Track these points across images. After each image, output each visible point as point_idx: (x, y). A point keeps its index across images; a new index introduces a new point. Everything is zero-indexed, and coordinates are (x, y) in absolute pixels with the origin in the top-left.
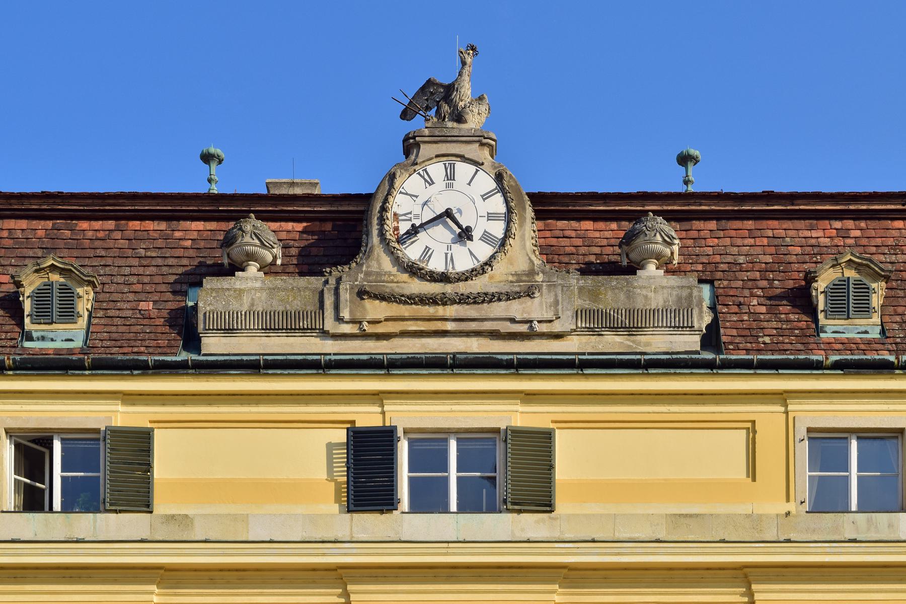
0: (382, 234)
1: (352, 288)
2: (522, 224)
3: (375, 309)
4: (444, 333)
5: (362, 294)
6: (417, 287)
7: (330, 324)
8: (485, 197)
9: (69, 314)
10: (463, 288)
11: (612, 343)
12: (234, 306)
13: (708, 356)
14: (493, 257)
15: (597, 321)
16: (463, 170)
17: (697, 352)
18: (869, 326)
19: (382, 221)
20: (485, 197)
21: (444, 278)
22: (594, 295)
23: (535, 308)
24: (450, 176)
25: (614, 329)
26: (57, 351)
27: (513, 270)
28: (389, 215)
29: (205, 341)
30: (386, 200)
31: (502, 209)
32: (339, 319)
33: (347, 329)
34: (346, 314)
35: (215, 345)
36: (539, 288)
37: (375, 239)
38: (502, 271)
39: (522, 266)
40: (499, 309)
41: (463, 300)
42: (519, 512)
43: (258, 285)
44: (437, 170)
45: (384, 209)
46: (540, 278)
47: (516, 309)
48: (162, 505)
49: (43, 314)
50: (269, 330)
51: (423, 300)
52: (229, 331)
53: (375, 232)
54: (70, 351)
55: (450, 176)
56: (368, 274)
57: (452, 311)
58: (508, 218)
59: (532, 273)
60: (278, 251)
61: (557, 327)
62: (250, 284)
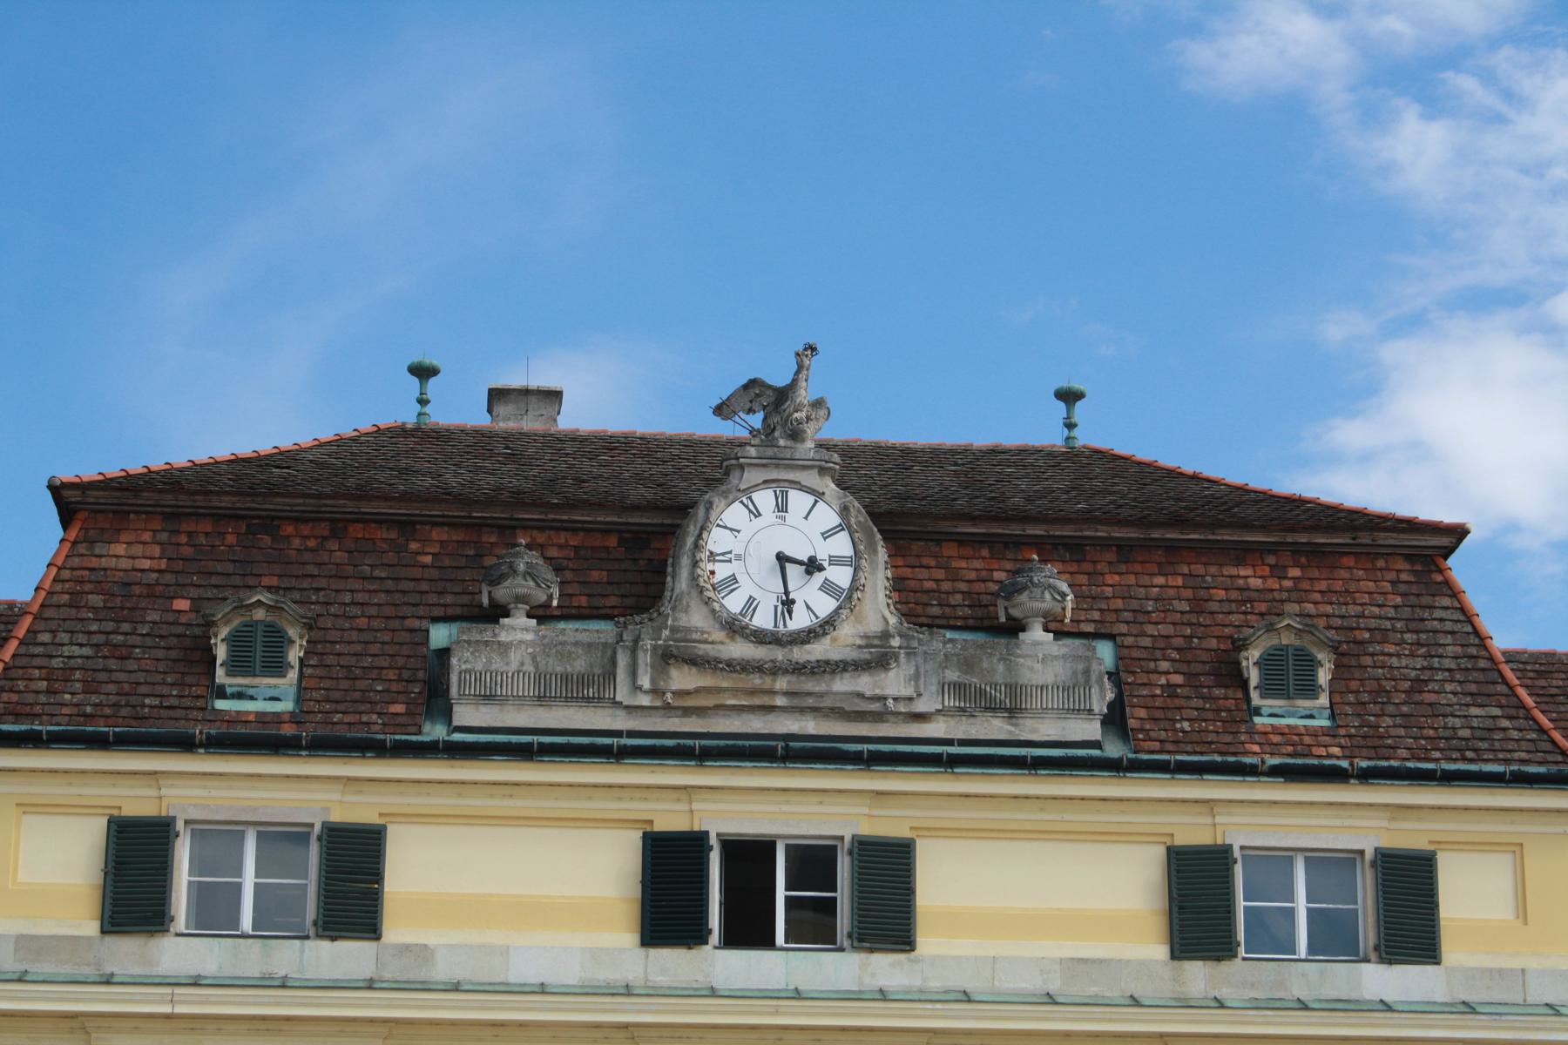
0: (694, 578)
1: (655, 648)
2: (874, 571)
3: (682, 679)
4: (772, 709)
5: (667, 658)
6: (740, 650)
7: (622, 694)
8: (826, 535)
9: (276, 666)
10: (801, 654)
11: (995, 727)
12: (498, 664)
13: (1114, 750)
14: (837, 612)
15: (973, 699)
16: (794, 495)
17: (1096, 745)
18: (1308, 714)
19: (695, 564)
20: (826, 535)
21: (760, 637)
22: (967, 665)
23: (894, 683)
24: (782, 507)
25: (992, 708)
26: (262, 717)
27: (861, 629)
28: (704, 555)
29: (456, 708)
30: (700, 536)
31: (848, 551)
32: (637, 688)
33: (645, 701)
34: (645, 681)
35: (465, 714)
36: (896, 657)
37: (683, 583)
38: (847, 632)
39: (873, 625)
40: (842, 685)
41: (799, 669)
42: (872, 950)
43: (529, 637)
44: (765, 499)
45: (697, 547)
46: (896, 642)
47: (865, 683)
48: (395, 930)
49: (238, 665)
50: (542, 699)
51: (746, 667)
52: (489, 698)
53: (684, 573)
54: (277, 718)
55: (782, 507)
56: (674, 630)
57: (782, 683)
58: (855, 562)
59: (885, 635)
60: (556, 591)
61: (921, 706)
62: (520, 636)
